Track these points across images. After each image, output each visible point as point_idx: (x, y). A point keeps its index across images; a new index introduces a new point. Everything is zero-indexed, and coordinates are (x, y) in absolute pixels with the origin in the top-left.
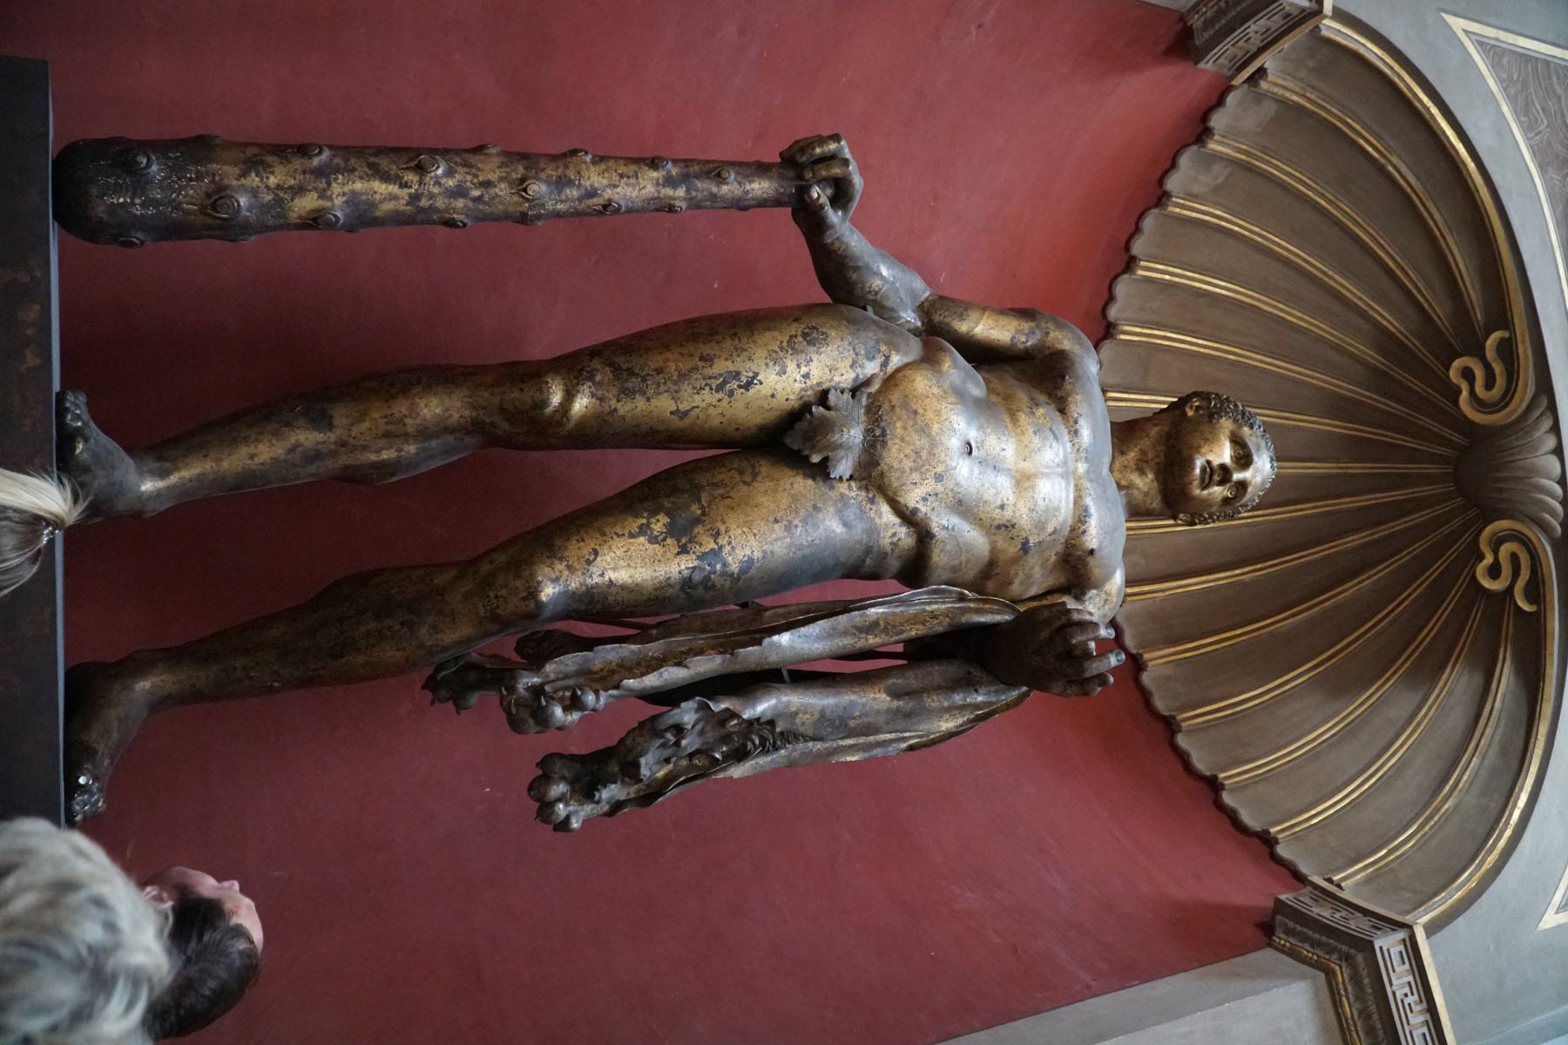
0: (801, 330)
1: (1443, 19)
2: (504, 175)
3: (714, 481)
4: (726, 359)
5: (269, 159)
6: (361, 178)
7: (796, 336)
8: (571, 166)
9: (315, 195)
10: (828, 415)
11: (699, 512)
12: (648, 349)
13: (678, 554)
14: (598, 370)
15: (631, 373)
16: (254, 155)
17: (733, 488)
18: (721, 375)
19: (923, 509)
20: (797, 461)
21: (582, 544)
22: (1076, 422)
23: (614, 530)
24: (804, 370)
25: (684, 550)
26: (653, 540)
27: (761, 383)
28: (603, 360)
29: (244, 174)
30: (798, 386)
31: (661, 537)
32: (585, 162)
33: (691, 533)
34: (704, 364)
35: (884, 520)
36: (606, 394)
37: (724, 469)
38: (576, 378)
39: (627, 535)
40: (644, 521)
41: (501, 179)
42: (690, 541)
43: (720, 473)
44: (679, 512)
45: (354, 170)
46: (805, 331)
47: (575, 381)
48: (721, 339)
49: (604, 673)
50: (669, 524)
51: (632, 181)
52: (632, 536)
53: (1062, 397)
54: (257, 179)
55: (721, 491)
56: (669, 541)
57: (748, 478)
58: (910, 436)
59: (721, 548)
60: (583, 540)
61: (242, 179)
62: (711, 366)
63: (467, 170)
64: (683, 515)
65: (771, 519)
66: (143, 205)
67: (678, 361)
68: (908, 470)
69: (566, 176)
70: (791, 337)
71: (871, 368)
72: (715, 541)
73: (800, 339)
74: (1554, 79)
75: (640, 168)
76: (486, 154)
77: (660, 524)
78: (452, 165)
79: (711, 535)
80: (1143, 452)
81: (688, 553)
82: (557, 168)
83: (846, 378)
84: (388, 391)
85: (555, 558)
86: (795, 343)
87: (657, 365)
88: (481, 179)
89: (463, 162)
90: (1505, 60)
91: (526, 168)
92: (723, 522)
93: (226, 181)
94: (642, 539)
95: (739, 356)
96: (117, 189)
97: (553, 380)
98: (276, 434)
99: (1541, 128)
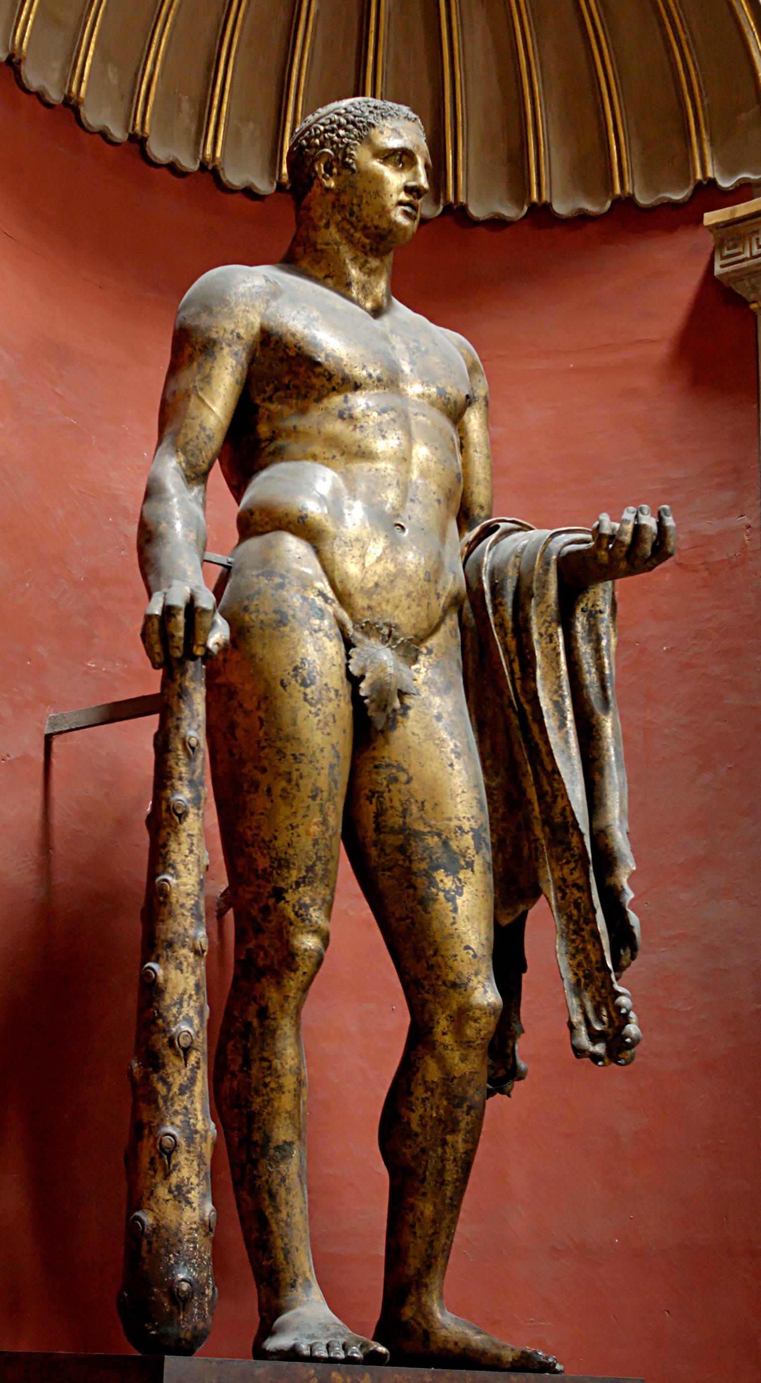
0: (297, 686)
2: (190, 969)
3: (400, 809)
4: (319, 774)
6: (192, 1103)
7: (305, 694)
8: (181, 901)
9: (204, 1145)
10: (370, 681)
11: (436, 839)
12: (289, 845)
13: (473, 871)
14: (300, 899)
15: (310, 869)
16: (170, 1191)
17: (413, 796)
18: (330, 784)
19: (443, 600)
21: (458, 958)
22: (370, 376)
23: (448, 925)
24: (332, 695)
25: (470, 865)
27: (338, 743)
28: (290, 891)
29: (189, 1203)
30: (343, 705)
31: (458, 882)
32: (177, 885)
33: (455, 853)
34: (319, 798)
35: (442, 641)
36: (321, 896)
37: (386, 795)
38: (303, 920)
39: (454, 915)
40: (441, 894)
41: (194, 973)
42: (464, 857)
43: (391, 801)
44: (434, 857)
45: (186, 1108)
46: (300, 681)
47: (307, 922)
48: (298, 773)
49: (581, 974)
50: (446, 871)
51: (195, 842)
52: (455, 910)
53: (343, 379)
54: (193, 1192)
55: (414, 809)
56: (461, 876)
57: (403, 777)
58: (394, 598)
59: (472, 830)
60: (456, 956)
61: (194, 1205)
62: (322, 791)
63: (185, 1004)
64: (438, 855)
65: (449, 769)
66: (208, 1288)
67: (310, 822)
68: (419, 609)
69: (191, 909)
70: (306, 700)
72: (467, 833)
73: (308, 691)
75: (184, 830)
76: (166, 981)
77: (446, 880)
78: (181, 1017)
79: (461, 835)
80: (354, 260)
81: (473, 861)
82: (183, 915)
84: (272, 1090)
85: (467, 984)
86: (312, 698)
87: (310, 842)
88: (193, 992)
89: (178, 1006)
91: (184, 946)
92: (450, 819)
93: (197, 1219)
94: (459, 901)
95: (318, 761)
96: (201, 1307)
97: (303, 943)
98: (288, 1190)
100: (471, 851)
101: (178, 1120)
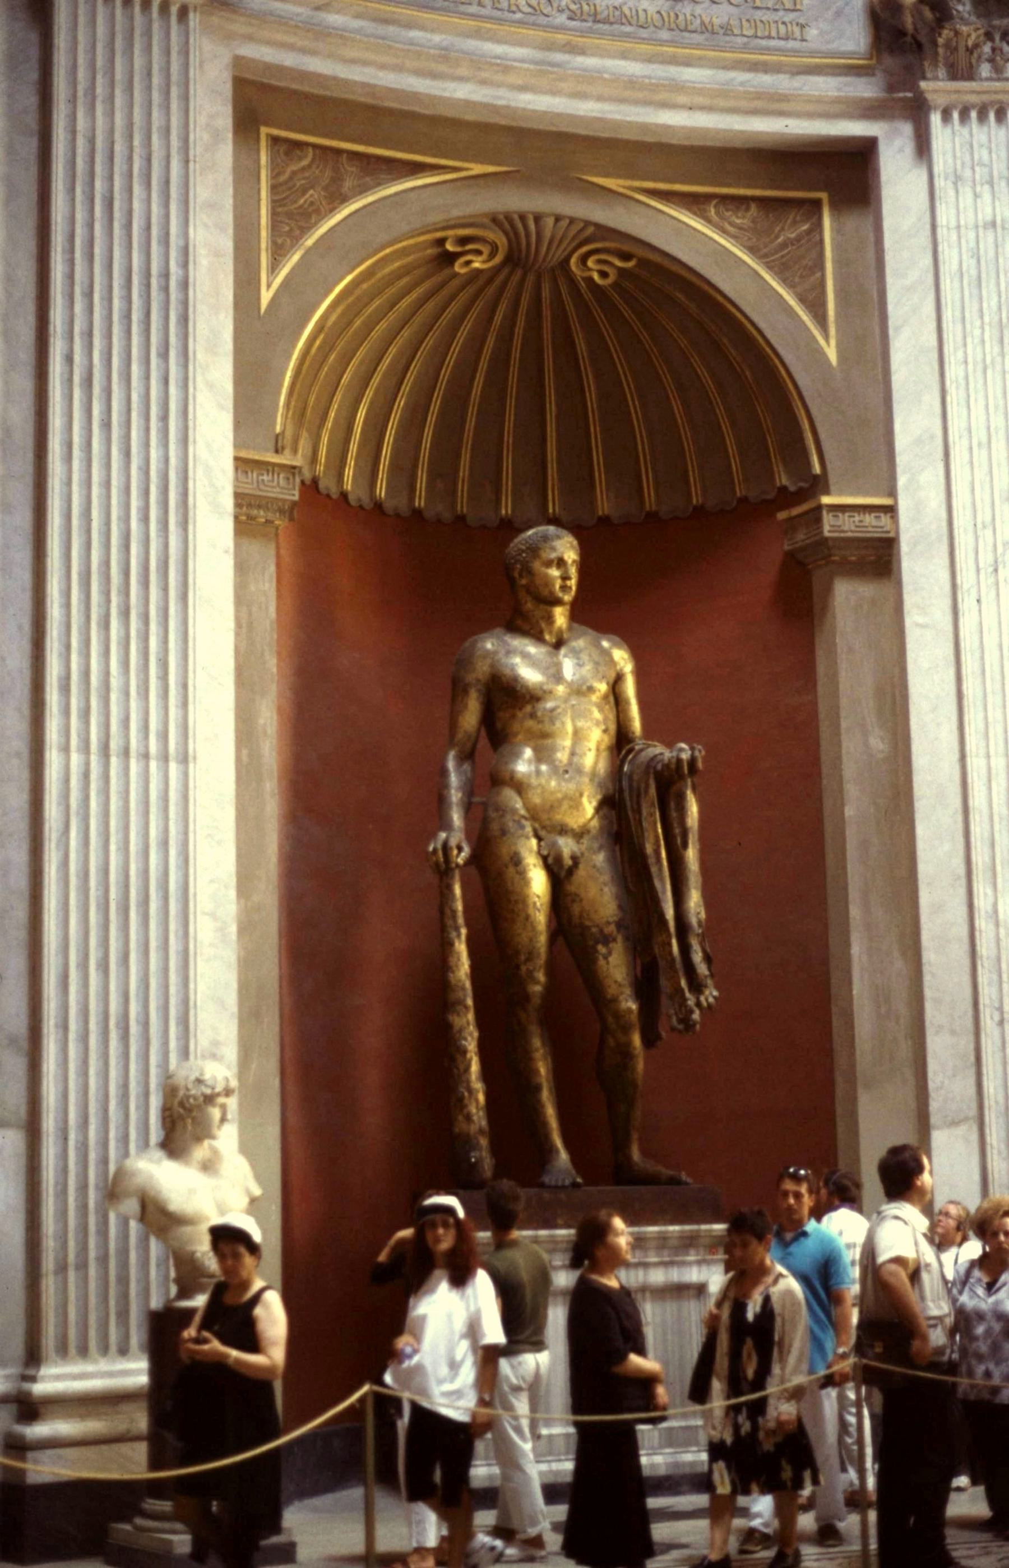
1: (266, 310)
5: (465, 1111)
20: (571, 871)
26: (610, 953)
29: (473, 1122)
56: (611, 945)
71: (529, 830)
74: (282, 178)
83: (534, 842)
90: (280, 241)
99: (316, 196)
100: (615, 932)
101: (465, 1085)
